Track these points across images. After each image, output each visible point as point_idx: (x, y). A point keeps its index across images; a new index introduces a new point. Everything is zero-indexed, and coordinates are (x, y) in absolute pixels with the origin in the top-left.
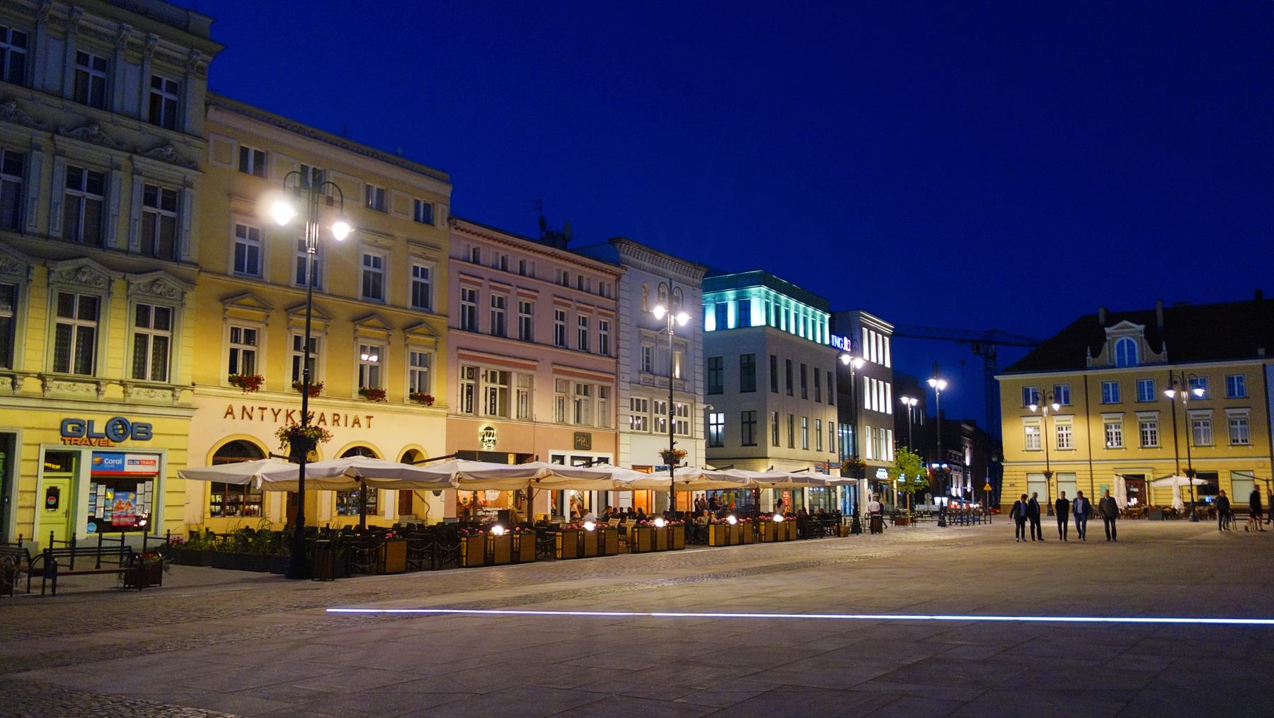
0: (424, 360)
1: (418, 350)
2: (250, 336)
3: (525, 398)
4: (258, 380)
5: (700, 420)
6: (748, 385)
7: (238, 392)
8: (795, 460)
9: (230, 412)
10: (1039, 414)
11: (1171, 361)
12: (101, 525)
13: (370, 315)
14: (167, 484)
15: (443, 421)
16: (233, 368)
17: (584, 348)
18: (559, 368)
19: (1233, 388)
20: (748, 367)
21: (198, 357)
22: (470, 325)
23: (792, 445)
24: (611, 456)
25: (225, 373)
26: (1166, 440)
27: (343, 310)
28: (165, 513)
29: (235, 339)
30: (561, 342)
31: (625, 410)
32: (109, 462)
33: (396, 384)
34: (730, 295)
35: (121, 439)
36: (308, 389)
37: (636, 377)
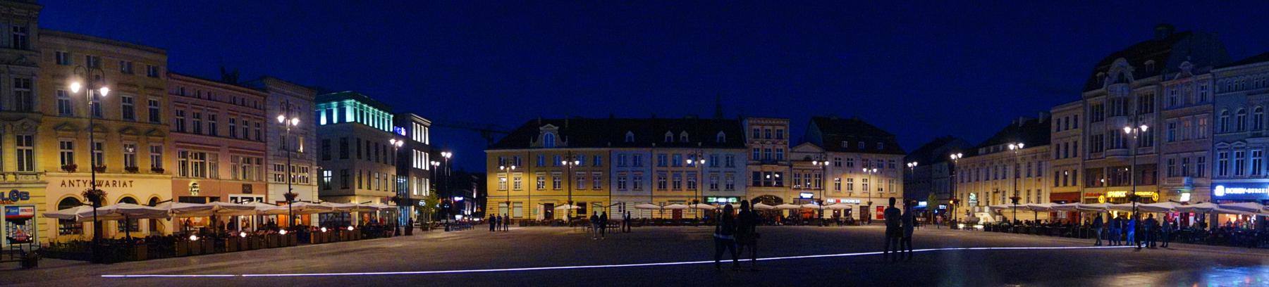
0: (158, 150)
2: (70, 145)
3: (214, 167)
4: (75, 167)
6: (344, 154)
8: (370, 197)
9: (63, 184)
10: (505, 171)
11: (570, 146)
12: (12, 240)
13: (128, 128)
14: (39, 220)
15: (169, 182)
16: (63, 162)
17: (246, 137)
18: (234, 150)
20: (344, 144)
21: (47, 159)
22: (182, 130)
24: (263, 196)
25: (59, 165)
26: (565, 186)
27: (114, 127)
28: (39, 234)
29: (62, 147)
30: (233, 135)
31: (271, 173)
32: (12, 211)
33: (144, 163)
35: (16, 200)
36: (98, 168)
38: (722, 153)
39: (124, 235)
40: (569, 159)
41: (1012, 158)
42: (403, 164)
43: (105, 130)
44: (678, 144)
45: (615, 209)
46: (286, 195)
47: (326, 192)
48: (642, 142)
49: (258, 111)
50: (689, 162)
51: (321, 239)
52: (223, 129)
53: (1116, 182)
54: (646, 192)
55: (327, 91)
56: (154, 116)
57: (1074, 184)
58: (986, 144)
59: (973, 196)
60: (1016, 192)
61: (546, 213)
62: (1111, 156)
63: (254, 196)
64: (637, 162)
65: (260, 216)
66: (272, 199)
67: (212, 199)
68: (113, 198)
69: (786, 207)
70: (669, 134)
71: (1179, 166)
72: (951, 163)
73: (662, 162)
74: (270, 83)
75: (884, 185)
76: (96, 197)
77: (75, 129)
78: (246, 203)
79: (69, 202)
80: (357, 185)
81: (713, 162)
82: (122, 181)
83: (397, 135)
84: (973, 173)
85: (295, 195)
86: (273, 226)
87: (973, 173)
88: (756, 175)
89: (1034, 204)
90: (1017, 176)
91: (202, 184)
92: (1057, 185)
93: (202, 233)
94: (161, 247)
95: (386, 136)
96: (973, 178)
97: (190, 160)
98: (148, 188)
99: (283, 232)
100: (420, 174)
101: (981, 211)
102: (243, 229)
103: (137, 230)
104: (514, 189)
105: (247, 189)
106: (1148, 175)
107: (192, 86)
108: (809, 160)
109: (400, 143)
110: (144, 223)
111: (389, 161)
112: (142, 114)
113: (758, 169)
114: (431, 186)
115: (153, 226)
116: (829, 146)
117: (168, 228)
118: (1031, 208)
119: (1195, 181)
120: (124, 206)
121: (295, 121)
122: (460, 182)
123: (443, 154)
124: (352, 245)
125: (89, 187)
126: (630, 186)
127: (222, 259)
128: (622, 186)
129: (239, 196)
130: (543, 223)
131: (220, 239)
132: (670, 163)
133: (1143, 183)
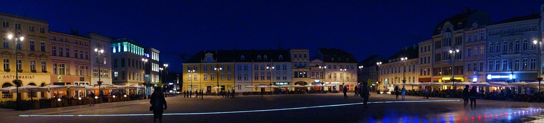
0: (45, 63)
1: (43, 61)
2: (8, 61)
3: (68, 70)
5: (111, 74)
6: (123, 65)
7: (6, 73)
8: (134, 83)
10: (190, 72)
15: (49, 76)
16: (5, 68)
17: (82, 58)
18: (77, 64)
19: (229, 68)
20: (123, 61)
22: (55, 54)
23: (134, 79)
25: (3, 69)
27: (26, 54)
29: (4, 62)
30: (76, 57)
31: (92, 72)
33: (39, 68)
34: (119, 44)
36: (19, 70)
37: (94, 64)
38: (281, 64)
39: (30, 99)
40: (218, 67)
41: (403, 64)
42: (148, 69)
43: (23, 55)
44: (263, 60)
45: (237, 88)
46: (98, 82)
47: (116, 81)
48: (248, 59)
49: (86, 47)
50: (268, 68)
51: (113, 100)
52: (72, 54)
53: (446, 74)
54: (250, 81)
55: (117, 38)
56: (43, 49)
57: (429, 74)
58: (392, 58)
59: (386, 80)
60: (404, 78)
61: (208, 90)
62: (444, 63)
63: (85, 82)
64: (246, 68)
65: (87, 91)
66: (92, 84)
67: (67, 84)
68: (25, 83)
69: (309, 86)
70: (259, 56)
71: (472, 67)
72: (377, 66)
73: (256, 68)
74: (92, 35)
75: (349, 76)
76: (18, 83)
77: (10, 54)
78: (82, 85)
79: (7, 85)
80: (128, 78)
81: (278, 68)
82: (29, 76)
83: (145, 57)
84: (386, 70)
85: (102, 82)
86: (93, 95)
87: (386, 70)
88: (296, 73)
89: (412, 83)
90: (405, 71)
91: (63, 78)
92: (421, 75)
93: (63, 98)
94: (46, 104)
95: (140, 57)
96: (386, 73)
97: (58, 67)
98: (41, 79)
99: (96, 97)
100: (155, 73)
101: (390, 86)
102: (80, 96)
103: (36, 97)
104: (194, 79)
105: (82, 79)
106: (459, 70)
107: (59, 36)
108: (318, 66)
109: (146, 60)
110: (39, 94)
111: (142, 67)
112: (38, 48)
113: (296, 70)
114: (160, 79)
115: (43, 95)
116: (326, 60)
117: (49, 96)
118: (411, 85)
119: (479, 73)
120: (30, 87)
121: (102, 51)
122: (172, 76)
123: (165, 65)
124: (126, 103)
125: (15, 78)
126: (243, 79)
127: (73, 109)
128: (240, 78)
129: (79, 82)
130: (206, 94)
131: (69, 101)
132: (260, 69)
133: (457, 74)
